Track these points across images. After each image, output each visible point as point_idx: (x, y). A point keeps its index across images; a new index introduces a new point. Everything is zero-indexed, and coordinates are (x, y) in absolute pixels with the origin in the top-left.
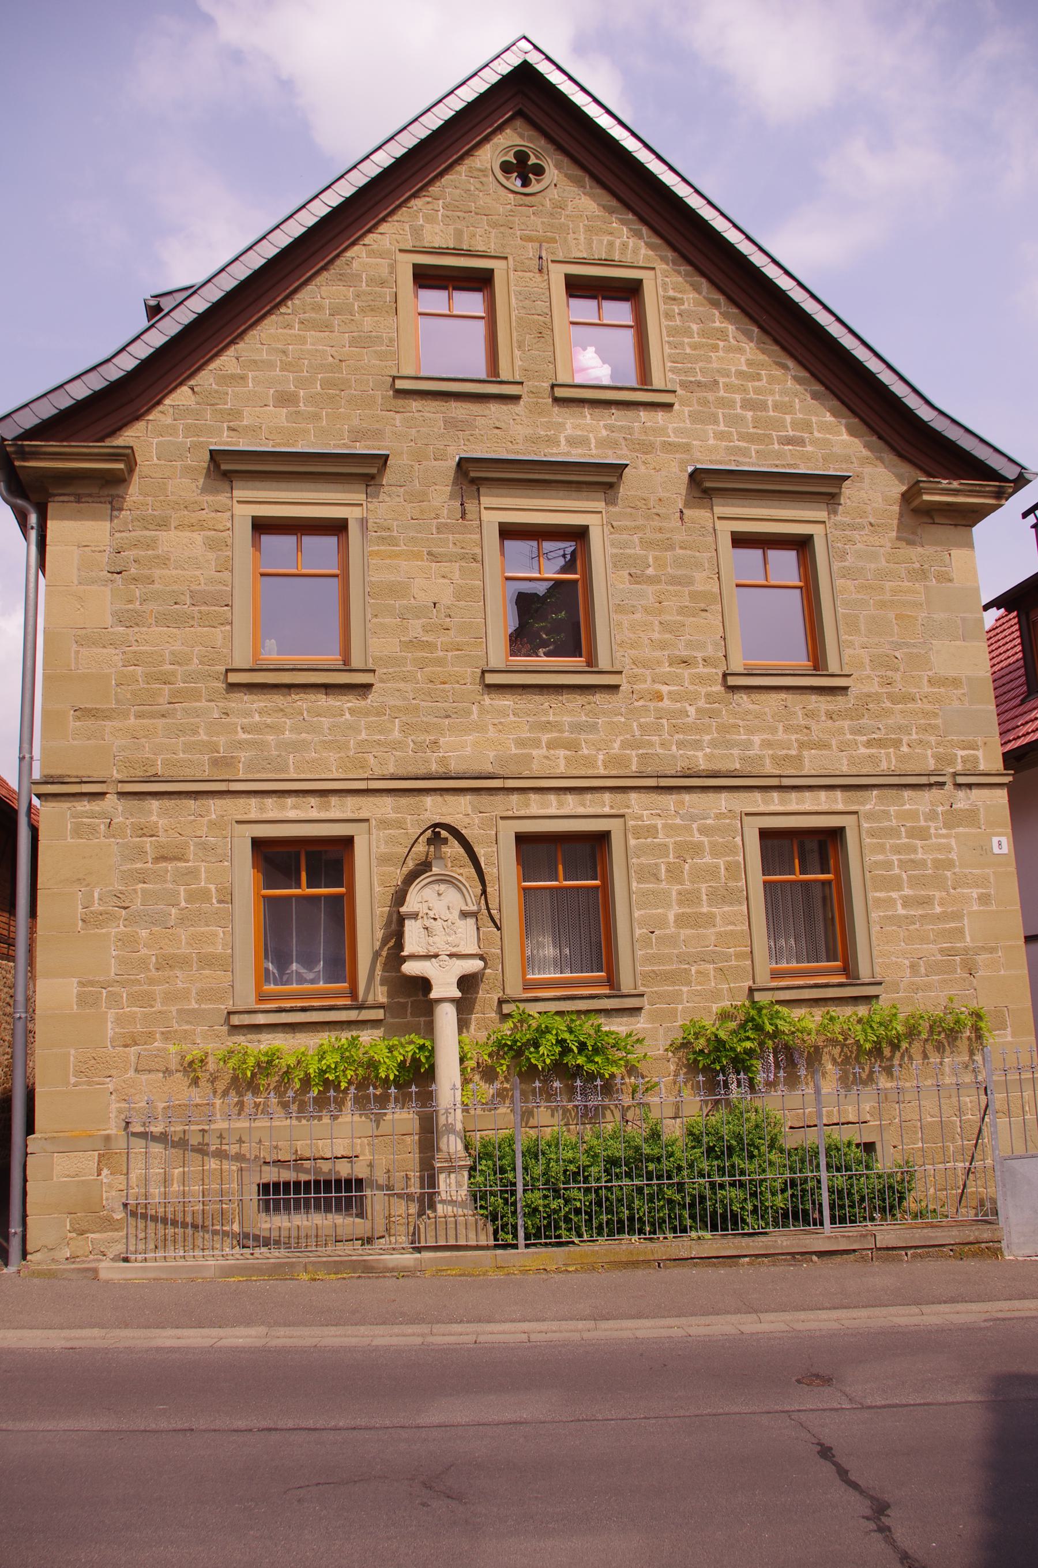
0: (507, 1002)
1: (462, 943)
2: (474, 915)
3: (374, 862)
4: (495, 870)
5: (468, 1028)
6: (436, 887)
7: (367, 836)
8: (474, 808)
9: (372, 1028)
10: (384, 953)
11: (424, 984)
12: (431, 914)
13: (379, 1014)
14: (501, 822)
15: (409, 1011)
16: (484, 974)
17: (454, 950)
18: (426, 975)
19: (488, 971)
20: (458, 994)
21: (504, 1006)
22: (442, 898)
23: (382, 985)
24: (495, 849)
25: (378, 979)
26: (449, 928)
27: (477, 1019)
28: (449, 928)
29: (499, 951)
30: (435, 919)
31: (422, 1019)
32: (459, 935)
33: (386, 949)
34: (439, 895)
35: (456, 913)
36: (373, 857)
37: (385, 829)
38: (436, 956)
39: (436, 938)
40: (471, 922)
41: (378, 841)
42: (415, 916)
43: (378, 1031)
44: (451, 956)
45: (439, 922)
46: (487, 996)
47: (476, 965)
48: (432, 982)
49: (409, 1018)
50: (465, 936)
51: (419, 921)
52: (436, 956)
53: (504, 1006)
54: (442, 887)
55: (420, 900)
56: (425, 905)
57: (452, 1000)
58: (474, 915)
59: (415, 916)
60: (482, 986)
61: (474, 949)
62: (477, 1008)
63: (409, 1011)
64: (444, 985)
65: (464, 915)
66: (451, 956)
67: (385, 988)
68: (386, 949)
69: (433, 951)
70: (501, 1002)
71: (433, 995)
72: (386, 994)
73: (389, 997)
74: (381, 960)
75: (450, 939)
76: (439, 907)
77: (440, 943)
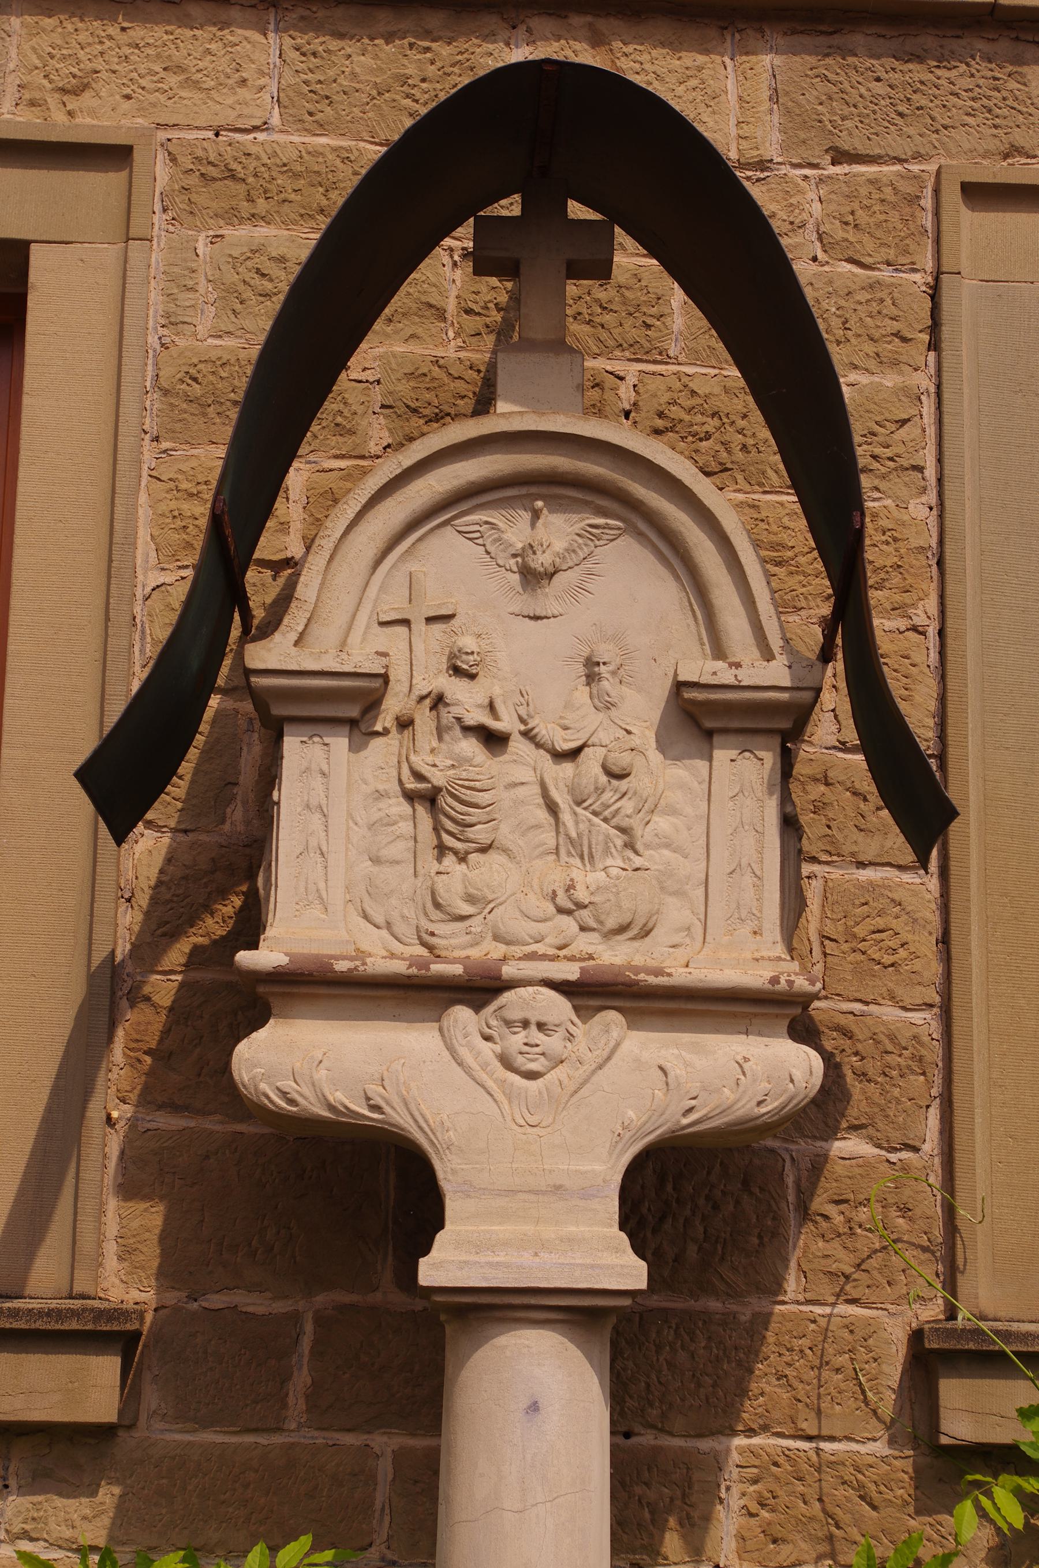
0: (984, 1359)
1: (676, 914)
2: (780, 725)
3: (144, 411)
4: (919, 509)
5: (696, 1528)
6: (514, 528)
7: (110, 253)
8: (797, 123)
9: (39, 1481)
10: (163, 987)
11: (383, 1184)
12: (468, 701)
13: (87, 1388)
14: (972, 228)
15: (302, 1379)
16: (818, 1165)
17: (615, 956)
18: (400, 1118)
19: (849, 1146)
20: (624, 1270)
21: (953, 1391)
22: (549, 599)
23: (129, 1189)
24: (924, 381)
25: (105, 1149)
26: (595, 802)
27: (763, 1468)
28: (595, 802)
29: (925, 1021)
30: (493, 740)
31: (385, 1443)
32: (653, 859)
33: (177, 955)
34: (533, 578)
35: (643, 708)
36: (140, 373)
37: (232, 216)
38: (481, 989)
39: (489, 872)
40: (742, 773)
41: (180, 282)
42: (353, 706)
43: (77, 1507)
44: (590, 993)
45: (522, 762)
46: (838, 1314)
47: (761, 1072)
48: (449, 1172)
49: (296, 1433)
50: (703, 867)
51: (382, 753)
52: (481, 989)
53: (953, 1391)
54: (557, 531)
55: (394, 605)
56: (431, 643)
57: (576, 1312)
58: (780, 725)
59: (353, 706)
60: (807, 1247)
61: (750, 958)
62: (766, 1389)
63: (302, 1379)
64: (531, 1196)
65: (699, 718)
66: (590, 993)
67: (150, 1217)
68: (177, 955)
69: (459, 952)
70: (931, 1360)
71: (439, 1268)
72: (151, 1253)
73: (176, 1267)
74: (138, 1027)
75: (588, 880)
76: (527, 665)
77: (515, 901)
